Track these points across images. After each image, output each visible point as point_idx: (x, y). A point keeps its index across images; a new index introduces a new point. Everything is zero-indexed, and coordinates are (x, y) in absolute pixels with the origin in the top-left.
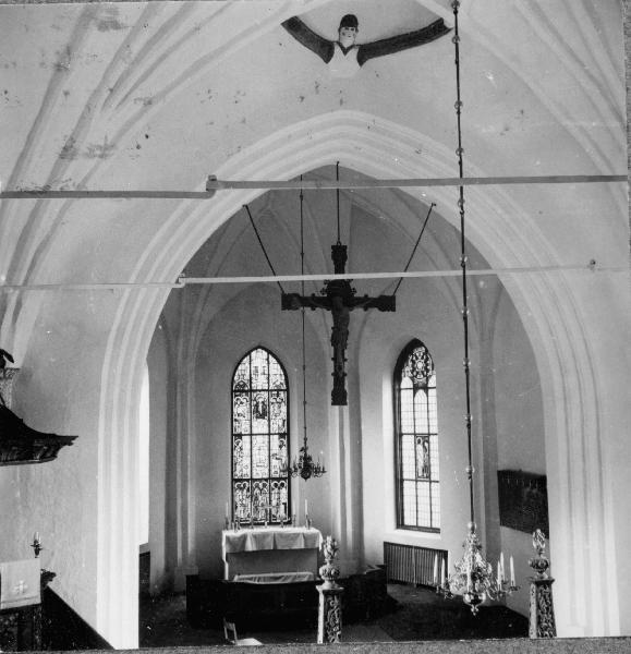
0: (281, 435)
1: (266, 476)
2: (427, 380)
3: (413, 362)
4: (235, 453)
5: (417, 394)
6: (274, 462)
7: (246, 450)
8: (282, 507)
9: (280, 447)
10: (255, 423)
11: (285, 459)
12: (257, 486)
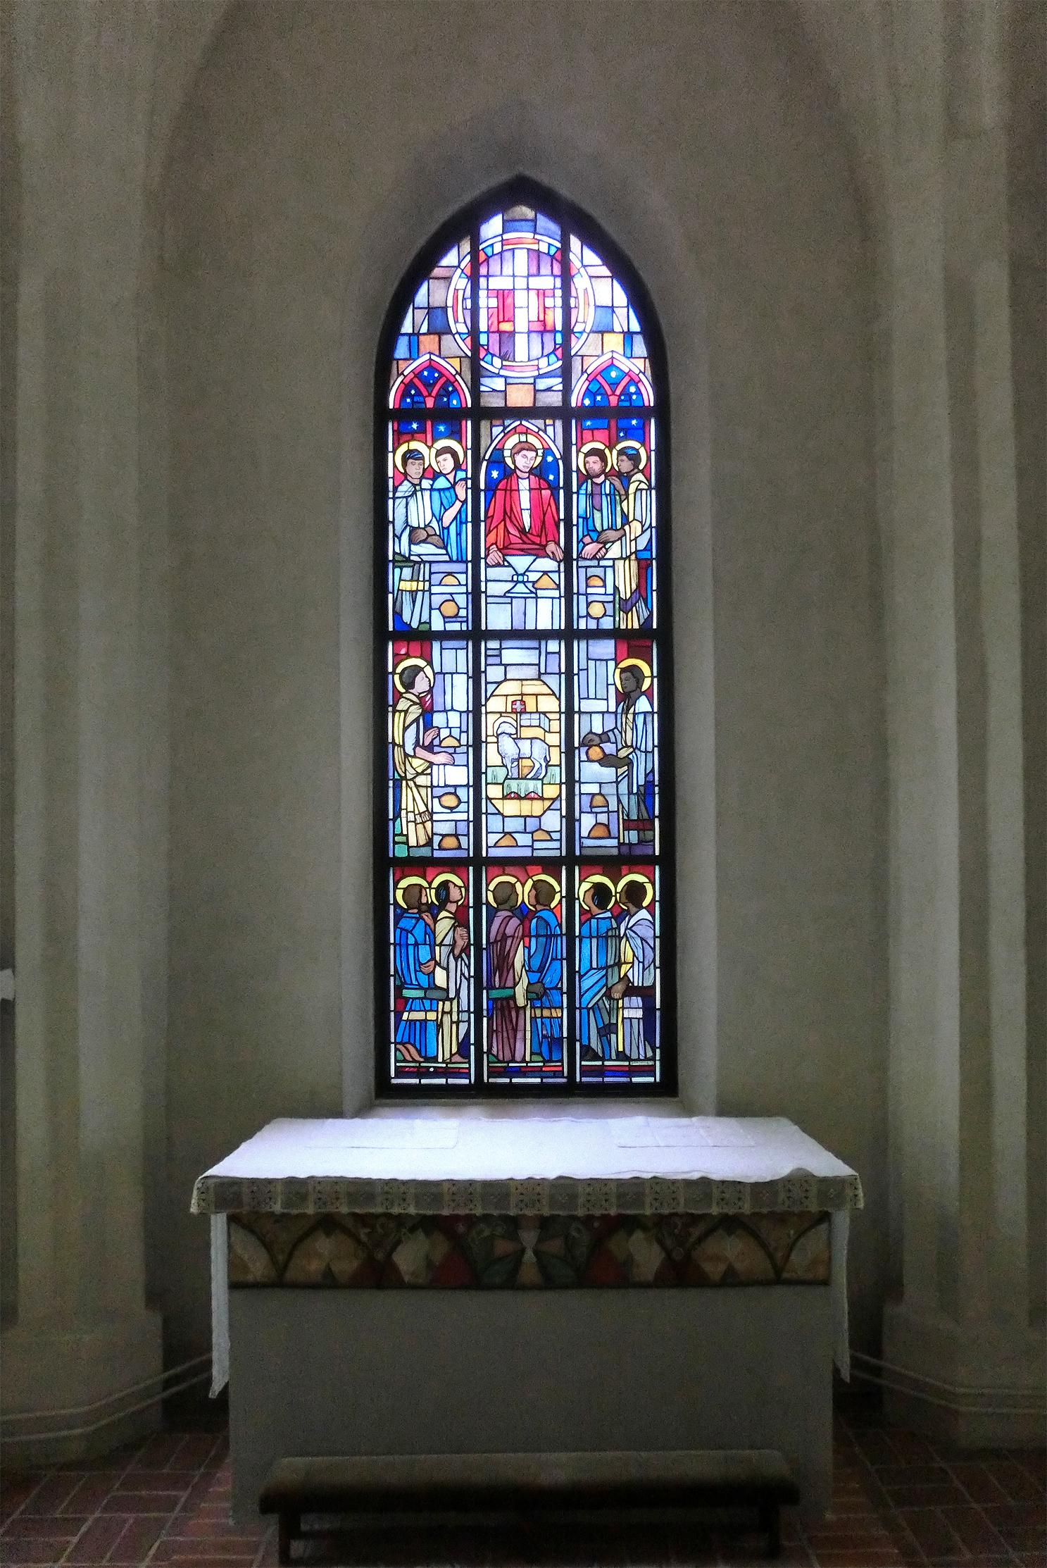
0: (631, 642)
4: (400, 729)
6: (592, 774)
7: (450, 722)
8: (633, 1010)
9: (626, 698)
10: (496, 581)
11: (646, 765)
12: (506, 896)
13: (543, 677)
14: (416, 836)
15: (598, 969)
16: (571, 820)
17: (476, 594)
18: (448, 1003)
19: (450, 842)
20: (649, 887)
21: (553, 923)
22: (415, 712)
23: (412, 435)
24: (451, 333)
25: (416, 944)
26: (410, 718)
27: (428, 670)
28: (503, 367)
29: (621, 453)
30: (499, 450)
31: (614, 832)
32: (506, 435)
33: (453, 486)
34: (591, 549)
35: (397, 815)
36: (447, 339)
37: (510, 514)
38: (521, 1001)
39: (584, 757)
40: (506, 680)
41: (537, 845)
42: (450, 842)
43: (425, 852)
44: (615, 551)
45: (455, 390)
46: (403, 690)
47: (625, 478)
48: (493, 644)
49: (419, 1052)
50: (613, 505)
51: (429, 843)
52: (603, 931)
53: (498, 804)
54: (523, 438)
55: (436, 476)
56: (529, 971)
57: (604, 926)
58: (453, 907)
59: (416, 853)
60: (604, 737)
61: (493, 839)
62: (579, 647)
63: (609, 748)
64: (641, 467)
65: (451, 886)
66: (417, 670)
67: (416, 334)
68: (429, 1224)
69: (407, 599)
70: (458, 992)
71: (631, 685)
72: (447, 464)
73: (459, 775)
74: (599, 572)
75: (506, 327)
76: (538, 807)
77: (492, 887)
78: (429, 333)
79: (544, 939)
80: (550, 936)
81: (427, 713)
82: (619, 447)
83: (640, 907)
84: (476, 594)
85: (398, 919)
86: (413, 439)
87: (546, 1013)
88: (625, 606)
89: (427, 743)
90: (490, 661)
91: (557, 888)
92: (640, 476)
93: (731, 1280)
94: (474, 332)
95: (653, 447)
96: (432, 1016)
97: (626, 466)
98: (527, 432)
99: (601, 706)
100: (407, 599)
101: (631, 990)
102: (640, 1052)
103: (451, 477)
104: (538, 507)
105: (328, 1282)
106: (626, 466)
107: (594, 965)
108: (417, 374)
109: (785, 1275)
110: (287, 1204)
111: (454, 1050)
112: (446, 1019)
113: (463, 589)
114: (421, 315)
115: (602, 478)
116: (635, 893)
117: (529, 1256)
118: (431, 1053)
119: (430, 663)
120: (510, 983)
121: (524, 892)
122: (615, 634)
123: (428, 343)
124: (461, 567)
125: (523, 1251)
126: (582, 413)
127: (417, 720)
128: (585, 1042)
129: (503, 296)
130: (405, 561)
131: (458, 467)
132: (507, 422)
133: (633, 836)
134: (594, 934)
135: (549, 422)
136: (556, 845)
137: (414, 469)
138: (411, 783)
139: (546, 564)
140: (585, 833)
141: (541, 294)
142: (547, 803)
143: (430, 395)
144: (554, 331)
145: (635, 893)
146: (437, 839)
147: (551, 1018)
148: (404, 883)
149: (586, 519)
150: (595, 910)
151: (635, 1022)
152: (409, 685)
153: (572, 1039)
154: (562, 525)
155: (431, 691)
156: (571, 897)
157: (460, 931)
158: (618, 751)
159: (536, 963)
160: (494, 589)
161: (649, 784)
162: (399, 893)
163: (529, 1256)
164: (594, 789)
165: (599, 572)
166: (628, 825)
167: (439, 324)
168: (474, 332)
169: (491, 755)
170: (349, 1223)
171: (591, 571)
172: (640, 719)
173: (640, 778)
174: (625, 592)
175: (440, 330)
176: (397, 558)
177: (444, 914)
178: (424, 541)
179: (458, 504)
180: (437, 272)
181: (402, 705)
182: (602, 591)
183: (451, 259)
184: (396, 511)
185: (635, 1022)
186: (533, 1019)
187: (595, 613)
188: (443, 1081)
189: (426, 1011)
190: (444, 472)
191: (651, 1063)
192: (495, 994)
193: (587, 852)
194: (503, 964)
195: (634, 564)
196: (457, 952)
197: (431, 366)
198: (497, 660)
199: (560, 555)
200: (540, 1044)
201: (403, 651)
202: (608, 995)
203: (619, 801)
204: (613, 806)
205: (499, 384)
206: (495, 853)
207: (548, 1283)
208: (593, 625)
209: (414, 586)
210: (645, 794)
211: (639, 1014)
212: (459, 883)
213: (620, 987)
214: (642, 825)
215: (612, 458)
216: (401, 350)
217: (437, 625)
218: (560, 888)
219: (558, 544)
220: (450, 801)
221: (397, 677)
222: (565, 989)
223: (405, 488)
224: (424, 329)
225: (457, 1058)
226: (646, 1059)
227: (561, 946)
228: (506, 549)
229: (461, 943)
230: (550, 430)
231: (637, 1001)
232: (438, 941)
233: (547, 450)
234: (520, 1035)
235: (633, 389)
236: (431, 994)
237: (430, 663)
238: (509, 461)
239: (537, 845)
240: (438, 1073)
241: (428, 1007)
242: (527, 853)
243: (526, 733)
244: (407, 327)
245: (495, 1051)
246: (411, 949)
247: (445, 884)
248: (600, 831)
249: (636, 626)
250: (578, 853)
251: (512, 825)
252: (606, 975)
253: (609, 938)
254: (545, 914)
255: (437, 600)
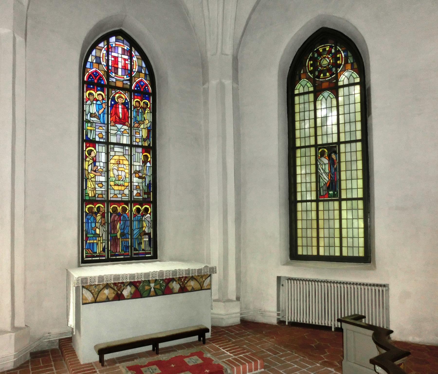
1: (126, 198)
2: (337, 79)
3: (314, 60)
5: (321, 97)
6: (135, 180)
7: (101, 165)
9: (145, 162)
10: (113, 130)
12: (115, 210)
13: (125, 156)
14: (91, 194)
15: (138, 228)
16: (131, 192)
17: (107, 133)
18: (100, 238)
19: (100, 196)
20: (150, 209)
21: (127, 217)
22: (91, 161)
23: (91, 89)
24: (101, 64)
25: (91, 223)
26: (90, 163)
27: (95, 151)
28: (115, 76)
29: (144, 102)
30: (114, 97)
31: (141, 195)
32: (116, 94)
33: (102, 104)
34: (136, 125)
35: (86, 188)
36: (100, 65)
37: (117, 114)
38: (119, 237)
39: (134, 176)
40: (115, 155)
41: (123, 197)
42: (100, 196)
43: (94, 198)
44: (142, 126)
45: (102, 79)
46: (87, 155)
47: (145, 109)
48: (112, 146)
49: (92, 251)
50: (142, 115)
51: (95, 196)
52: (139, 219)
53: (113, 187)
54: (120, 95)
55: (97, 100)
56: (121, 229)
57: (139, 218)
58: (101, 213)
59: (91, 198)
60: (139, 172)
61: (112, 195)
62: (133, 149)
63: (140, 174)
64: (148, 107)
65: (101, 207)
66: (92, 151)
67: (92, 62)
68: (131, 284)
69: (89, 132)
70: (102, 235)
71: (146, 159)
72: (101, 98)
73: (103, 179)
74: (138, 131)
75: (116, 66)
76: (123, 188)
77: (111, 208)
78: (96, 63)
79: (124, 221)
80: (126, 221)
81: (95, 162)
82: (143, 101)
83: (148, 213)
84: (107, 133)
85: (86, 216)
86: (91, 90)
87: (125, 240)
88: (144, 140)
89: (94, 170)
90: (111, 150)
91: (128, 208)
92: (148, 109)
93: (193, 290)
94: (108, 65)
95: (151, 103)
96: (95, 241)
97: (145, 106)
98: (121, 93)
99: (138, 164)
100: (89, 132)
101: (145, 234)
102: (148, 248)
103: (101, 101)
104: (124, 113)
105: (108, 300)
106: (145, 106)
107: (137, 228)
108: (92, 73)
109: (203, 288)
110: (98, 282)
111: (101, 250)
112: (99, 242)
113: (104, 131)
114: (93, 58)
115: (139, 108)
116: (146, 210)
117: (152, 289)
118: (95, 251)
119: (95, 149)
120: (116, 232)
121: (119, 209)
122: (142, 146)
123: (95, 65)
124: (104, 125)
125: (151, 288)
126: (134, 91)
127: (92, 164)
128: (134, 247)
129: (116, 58)
130: (88, 121)
131: (103, 99)
132: (116, 90)
133: (146, 196)
134: (137, 220)
135: (126, 92)
136: (127, 198)
137: (91, 98)
138: (90, 180)
139: (125, 127)
140: (134, 195)
141: (125, 60)
142: (125, 187)
143: (96, 79)
144: (128, 70)
145: (146, 210)
146: (97, 195)
147: (126, 241)
148: (88, 206)
149: (135, 117)
150: (137, 214)
151: (146, 242)
152: (90, 154)
153: (132, 246)
154: (129, 118)
155: (95, 156)
156: (131, 210)
157: (103, 219)
158: (142, 175)
159: (123, 227)
160: (112, 132)
161: (150, 184)
162: (87, 209)
163: (152, 289)
164: (137, 184)
165: (138, 131)
166: (145, 193)
167: (98, 61)
168: (108, 65)
169: (111, 174)
170: (112, 286)
171: (136, 131)
172: (148, 168)
173: (147, 182)
174: (145, 137)
175: (99, 63)
176: (87, 120)
177: (99, 215)
178: (94, 117)
179: (103, 109)
180: (97, 47)
181: (88, 159)
182: (139, 136)
183: (102, 45)
184: (86, 108)
185: (146, 242)
186: (122, 242)
187: (137, 141)
188: (98, 258)
189: (94, 240)
190: (100, 100)
191: (150, 251)
192: (112, 235)
193: (135, 200)
194: (114, 227)
195: (147, 130)
196: (102, 224)
197: (96, 71)
198: (113, 150)
199: (129, 125)
200: (124, 248)
201: (88, 145)
202: (140, 235)
203: (143, 188)
204: (141, 188)
205: (114, 80)
206: (112, 199)
207: (156, 295)
208: (137, 144)
209: (91, 128)
210: (149, 186)
211: (147, 239)
212: (102, 206)
213: (143, 233)
214: (148, 193)
215: (142, 104)
216: (88, 66)
217: (97, 139)
218: (128, 208)
219: (128, 122)
220: (101, 185)
221: (86, 152)
222: (130, 234)
223: (89, 102)
224: (94, 61)
225: (102, 252)
226: (149, 250)
227: (128, 223)
228: (116, 122)
229: (103, 222)
230: (127, 94)
231: (147, 236)
232: (97, 222)
233: (126, 99)
234: (118, 246)
235: (147, 88)
236: (95, 236)
237: (95, 149)
238: (116, 100)
239: (123, 197)
240: (97, 256)
241: (94, 239)
242: (120, 199)
243: (120, 169)
244: (90, 60)
245: (112, 250)
246: (90, 224)
247: (99, 207)
248: (138, 195)
249: (147, 145)
250: (133, 200)
251: (116, 192)
252: (140, 230)
253: (140, 221)
254: (125, 215)
255: (97, 133)
